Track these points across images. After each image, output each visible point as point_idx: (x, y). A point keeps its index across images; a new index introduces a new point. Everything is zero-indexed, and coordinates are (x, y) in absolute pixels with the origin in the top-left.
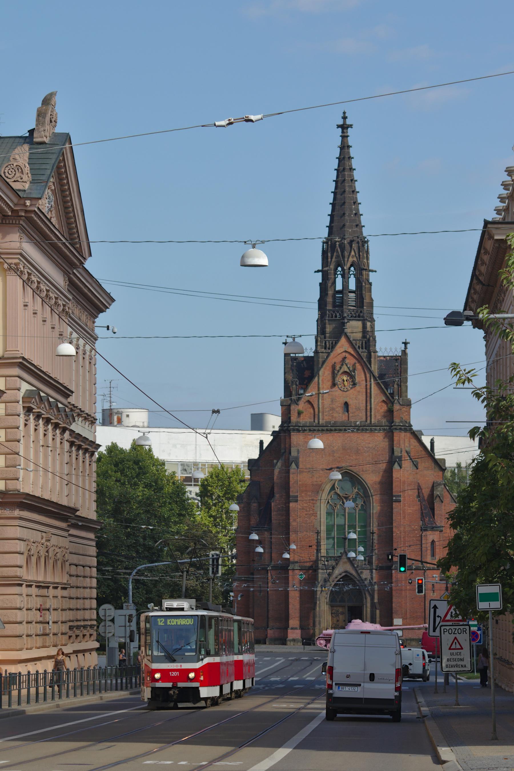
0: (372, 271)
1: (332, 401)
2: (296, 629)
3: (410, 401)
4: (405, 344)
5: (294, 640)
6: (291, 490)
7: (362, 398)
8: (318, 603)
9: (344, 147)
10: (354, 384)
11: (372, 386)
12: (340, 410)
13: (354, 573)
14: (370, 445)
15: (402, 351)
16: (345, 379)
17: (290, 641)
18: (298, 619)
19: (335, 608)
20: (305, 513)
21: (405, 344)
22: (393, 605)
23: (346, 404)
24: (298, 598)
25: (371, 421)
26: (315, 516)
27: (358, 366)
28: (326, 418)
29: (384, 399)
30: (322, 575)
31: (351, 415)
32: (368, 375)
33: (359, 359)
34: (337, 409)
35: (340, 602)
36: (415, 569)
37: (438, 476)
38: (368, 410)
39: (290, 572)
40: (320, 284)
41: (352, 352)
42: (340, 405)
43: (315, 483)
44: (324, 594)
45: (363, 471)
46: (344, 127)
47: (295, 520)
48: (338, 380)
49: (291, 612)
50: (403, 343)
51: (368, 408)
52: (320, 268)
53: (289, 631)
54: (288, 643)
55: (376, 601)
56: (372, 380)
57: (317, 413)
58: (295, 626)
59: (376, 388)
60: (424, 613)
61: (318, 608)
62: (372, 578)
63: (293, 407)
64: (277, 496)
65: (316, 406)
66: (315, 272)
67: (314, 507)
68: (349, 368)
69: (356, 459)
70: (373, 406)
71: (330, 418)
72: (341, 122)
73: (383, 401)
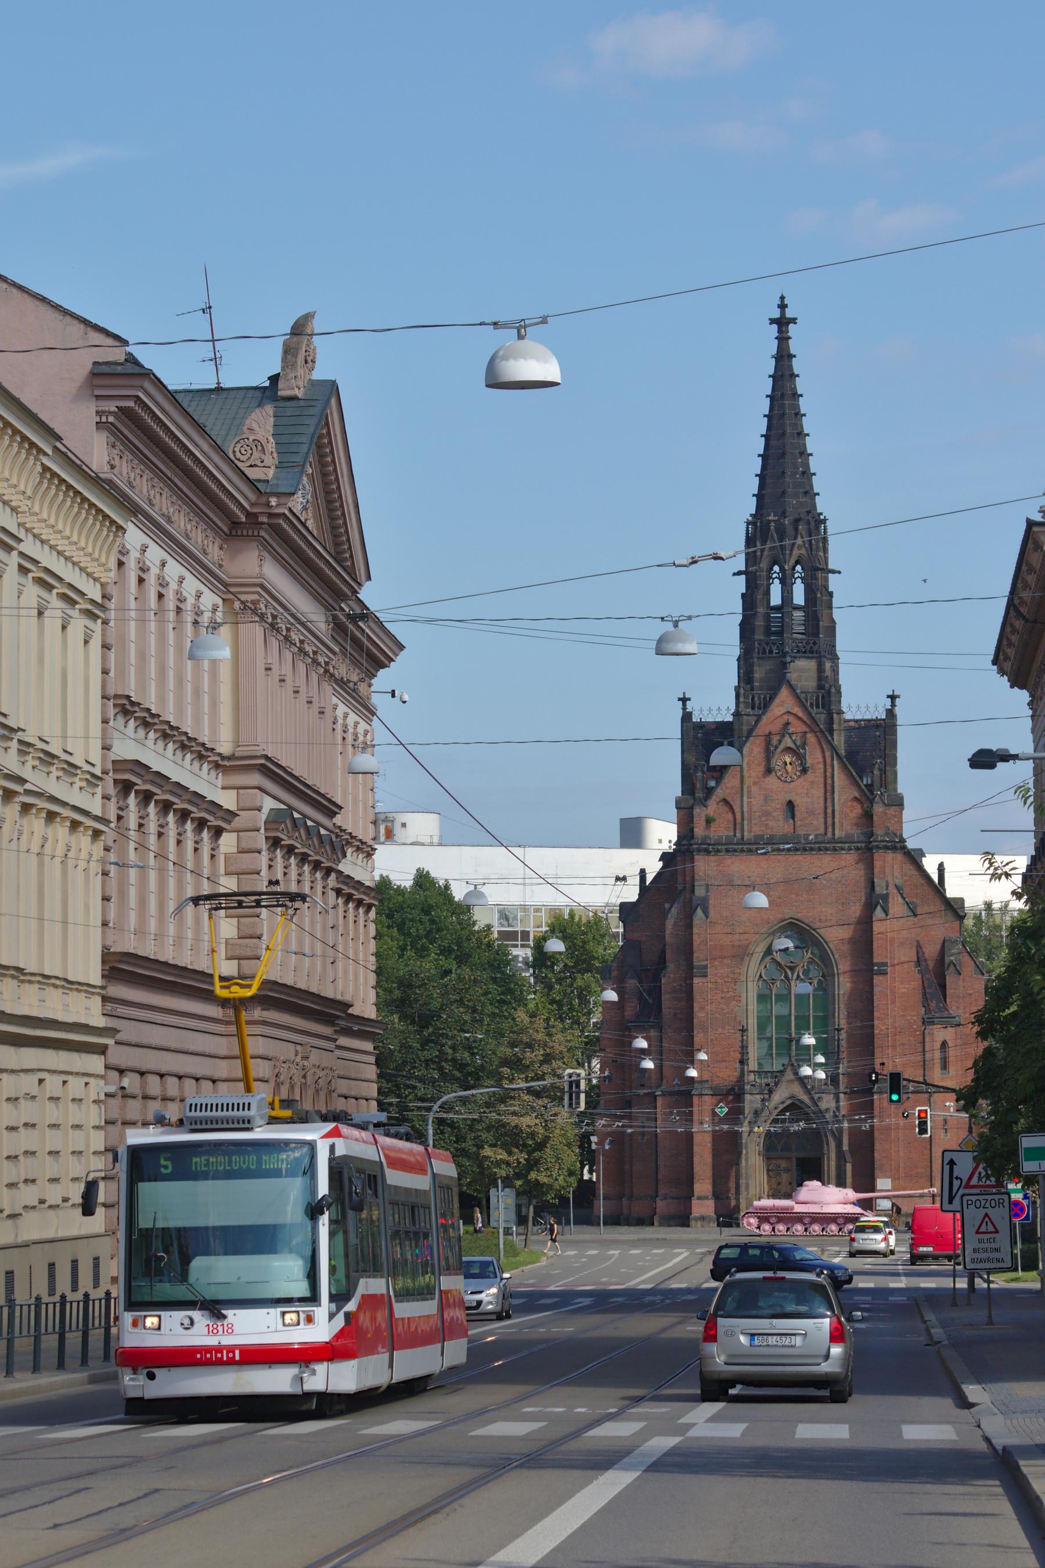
0: (834, 572)
1: (766, 800)
2: (706, 1198)
3: (902, 799)
4: (893, 698)
5: (702, 1218)
6: (695, 955)
7: (818, 793)
8: (744, 1152)
9: (783, 357)
10: (804, 771)
11: (836, 773)
13: (805, 1098)
15: (888, 711)
16: (788, 760)
17: (696, 1219)
18: (711, 1181)
19: (774, 1161)
20: (720, 995)
21: (893, 698)
23: (790, 805)
24: (709, 1145)
25: (834, 834)
27: (811, 738)
28: (755, 829)
29: (857, 794)
30: (751, 1102)
31: (798, 823)
32: (828, 754)
33: (813, 724)
34: (775, 814)
35: (782, 1150)
36: (912, 1092)
38: (829, 814)
39: (695, 1099)
40: (743, 595)
41: (800, 714)
44: (754, 1137)
46: (782, 323)
47: (702, 1009)
48: (777, 763)
49: (697, 1168)
50: (888, 696)
51: (829, 811)
52: (743, 568)
53: (695, 1202)
54: (693, 1223)
55: (845, 1147)
56: (835, 762)
57: (739, 820)
58: (703, 1194)
59: (843, 776)
60: (929, 1169)
61: (743, 1162)
62: (838, 1108)
63: (697, 811)
64: (671, 966)
65: (737, 809)
66: (734, 574)
68: (794, 742)
69: (809, 900)
70: (836, 808)
72: (776, 314)
73: (856, 799)
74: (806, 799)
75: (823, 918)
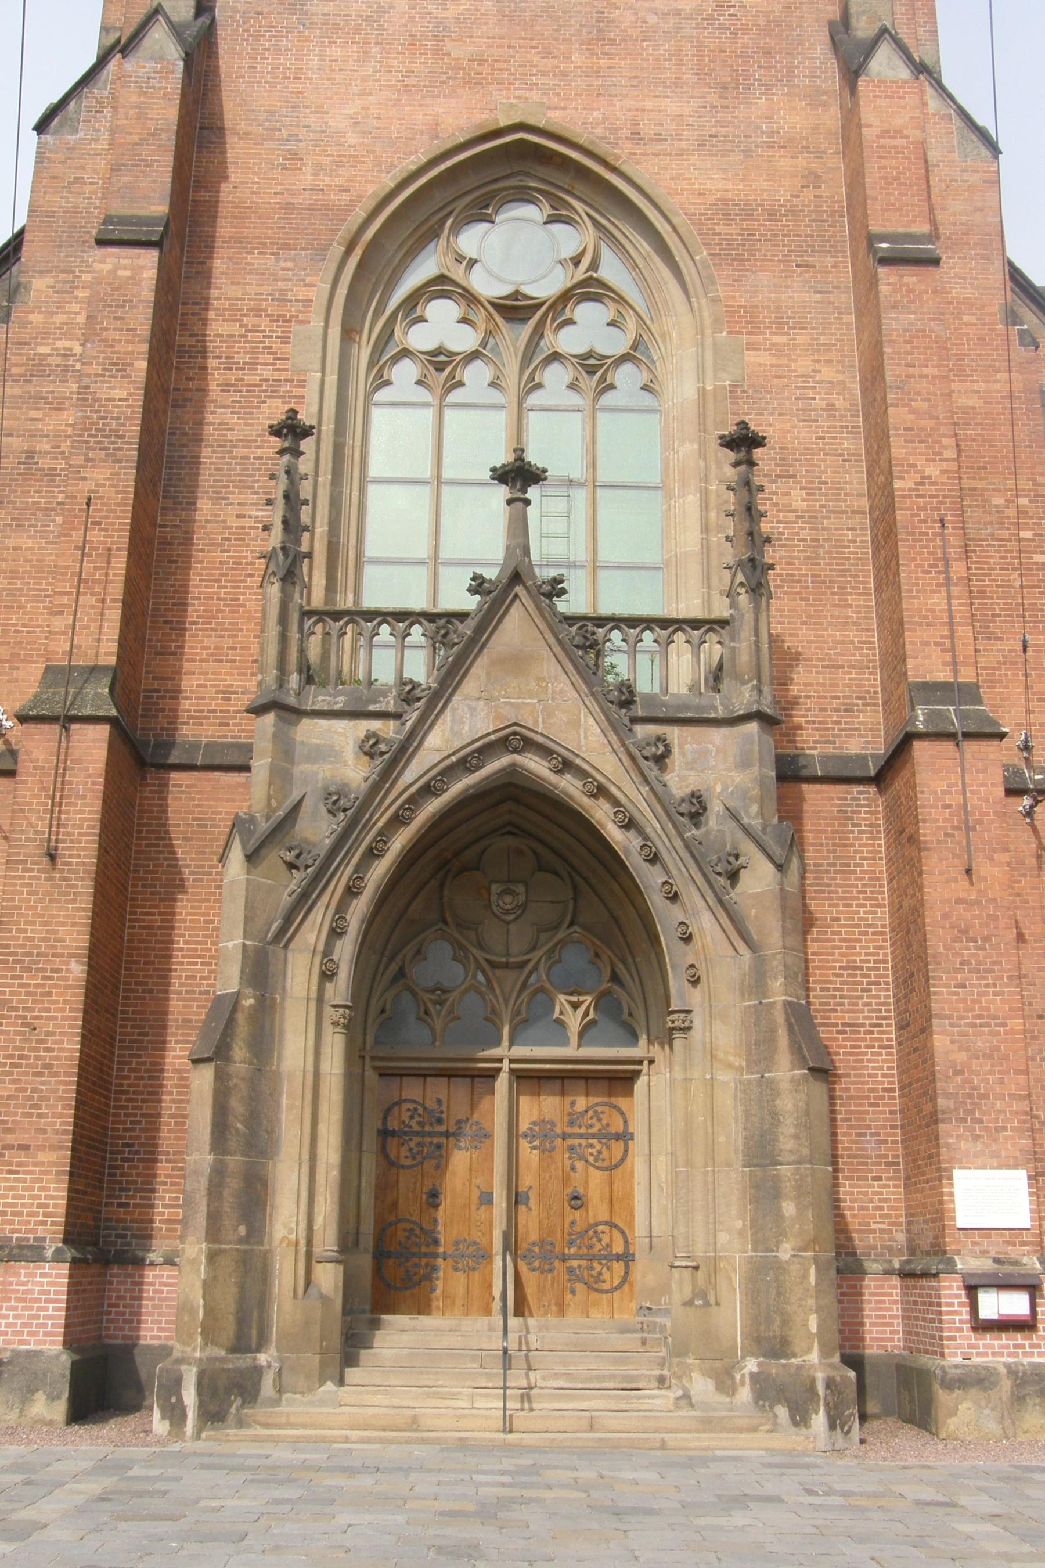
22: (940, 1042)
24: (77, 970)
43: (305, 199)
45: (636, 136)
67: (285, 340)
75: (648, 129)
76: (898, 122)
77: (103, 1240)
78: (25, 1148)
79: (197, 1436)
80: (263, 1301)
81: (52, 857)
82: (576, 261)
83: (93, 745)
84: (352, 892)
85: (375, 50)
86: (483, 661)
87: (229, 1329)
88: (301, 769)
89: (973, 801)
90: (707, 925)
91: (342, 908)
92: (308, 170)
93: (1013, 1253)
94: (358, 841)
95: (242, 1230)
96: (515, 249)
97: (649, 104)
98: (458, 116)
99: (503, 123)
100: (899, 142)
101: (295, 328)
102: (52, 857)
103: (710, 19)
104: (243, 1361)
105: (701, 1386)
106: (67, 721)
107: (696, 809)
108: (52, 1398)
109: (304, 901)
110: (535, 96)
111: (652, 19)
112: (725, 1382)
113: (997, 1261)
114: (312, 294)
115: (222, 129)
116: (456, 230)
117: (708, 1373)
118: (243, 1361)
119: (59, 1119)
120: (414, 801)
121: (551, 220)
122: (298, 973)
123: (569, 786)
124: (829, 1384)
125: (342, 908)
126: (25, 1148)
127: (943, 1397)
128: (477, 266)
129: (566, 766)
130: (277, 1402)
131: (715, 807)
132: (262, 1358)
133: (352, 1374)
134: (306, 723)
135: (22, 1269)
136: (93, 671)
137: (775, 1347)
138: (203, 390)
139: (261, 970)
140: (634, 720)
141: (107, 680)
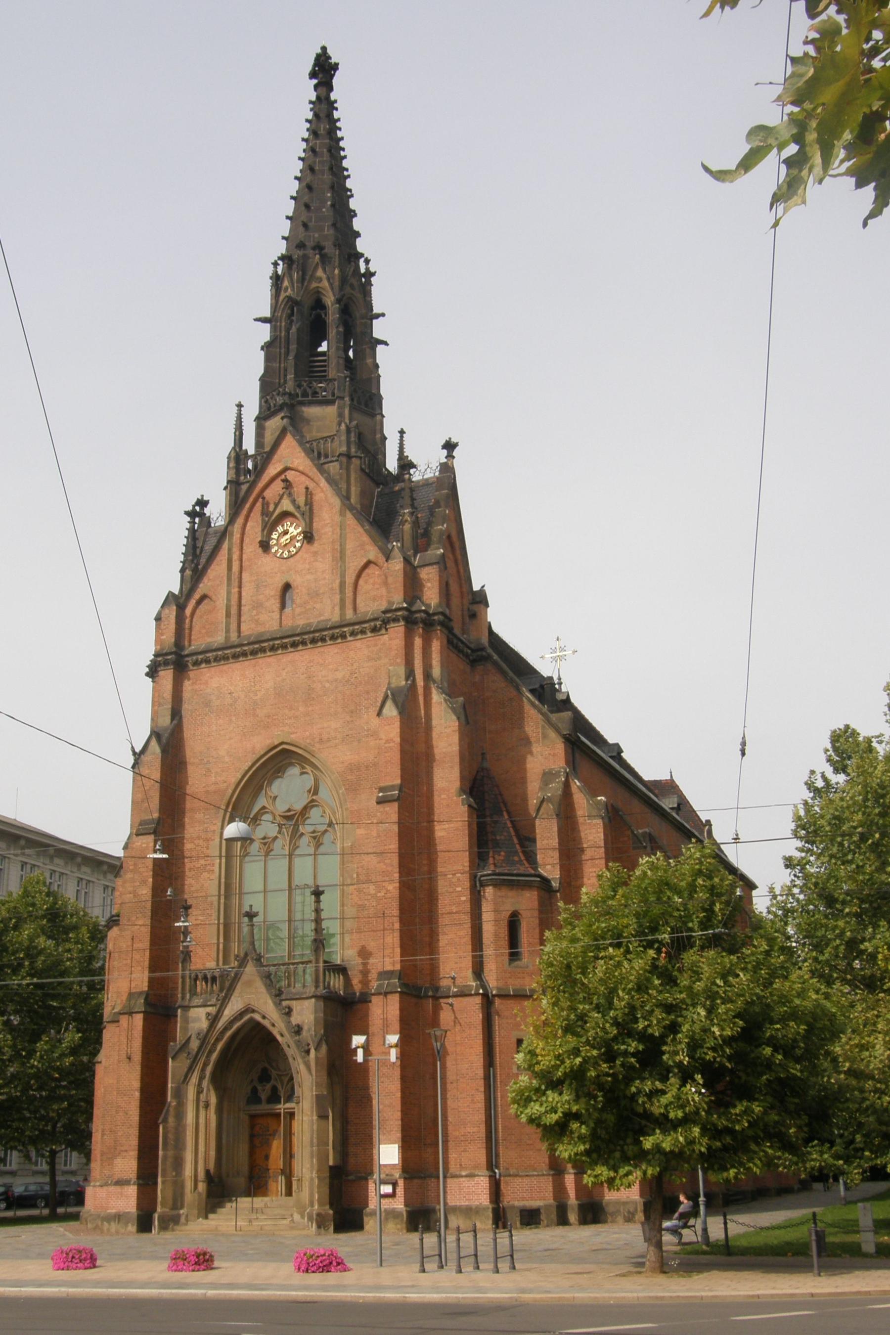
4: (450, 446)
12: (275, 604)
14: (339, 675)
21: (450, 446)
26: (209, 872)
36: (456, 996)
37: (554, 755)
42: (272, 593)
43: (212, 788)
45: (321, 741)
67: (207, 848)
71: (253, 626)
74: (309, 577)
76: (392, 735)
77: (147, 1177)
78: (126, 1151)
79: (159, 1233)
80: (182, 1195)
81: (129, 1058)
82: (309, 791)
83: (139, 1019)
84: (205, 1065)
85: (234, 718)
86: (239, 984)
87: (170, 1202)
88: (191, 1025)
89: (389, 1016)
90: (302, 1067)
91: (203, 1070)
92: (213, 775)
93: (393, 1172)
94: (206, 1047)
95: (174, 1174)
96: (289, 791)
97: (325, 725)
98: (261, 743)
99: (276, 743)
100: (392, 744)
101: (211, 843)
102: (129, 1058)
103: (348, 680)
104: (175, 1212)
105: (297, 1217)
106: (131, 1014)
107: (298, 1030)
108: (133, 1225)
109: (191, 1069)
110: (286, 729)
111: (327, 685)
112: (303, 1217)
113: (387, 1175)
114: (215, 828)
115: (186, 763)
116: (270, 784)
117: (298, 1213)
118: (175, 1212)
119: (134, 1142)
120: (223, 1032)
121: (302, 773)
122: (191, 1092)
123: (266, 1023)
124: (318, 1215)
125: (203, 1070)
126: (126, 1151)
127: (365, 1219)
128: (278, 799)
129: (264, 1017)
130: (186, 1224)
131: (305, 1028)
132: (182, 1212)
133: (211, 1216)
134: (192, 1009)
135: (126, 1188)
136: (141, 993)
137: (312, 1205)
138: (184, 872)
139: (179, 1094)
140: (281, 1000)
141: (144, 996)
